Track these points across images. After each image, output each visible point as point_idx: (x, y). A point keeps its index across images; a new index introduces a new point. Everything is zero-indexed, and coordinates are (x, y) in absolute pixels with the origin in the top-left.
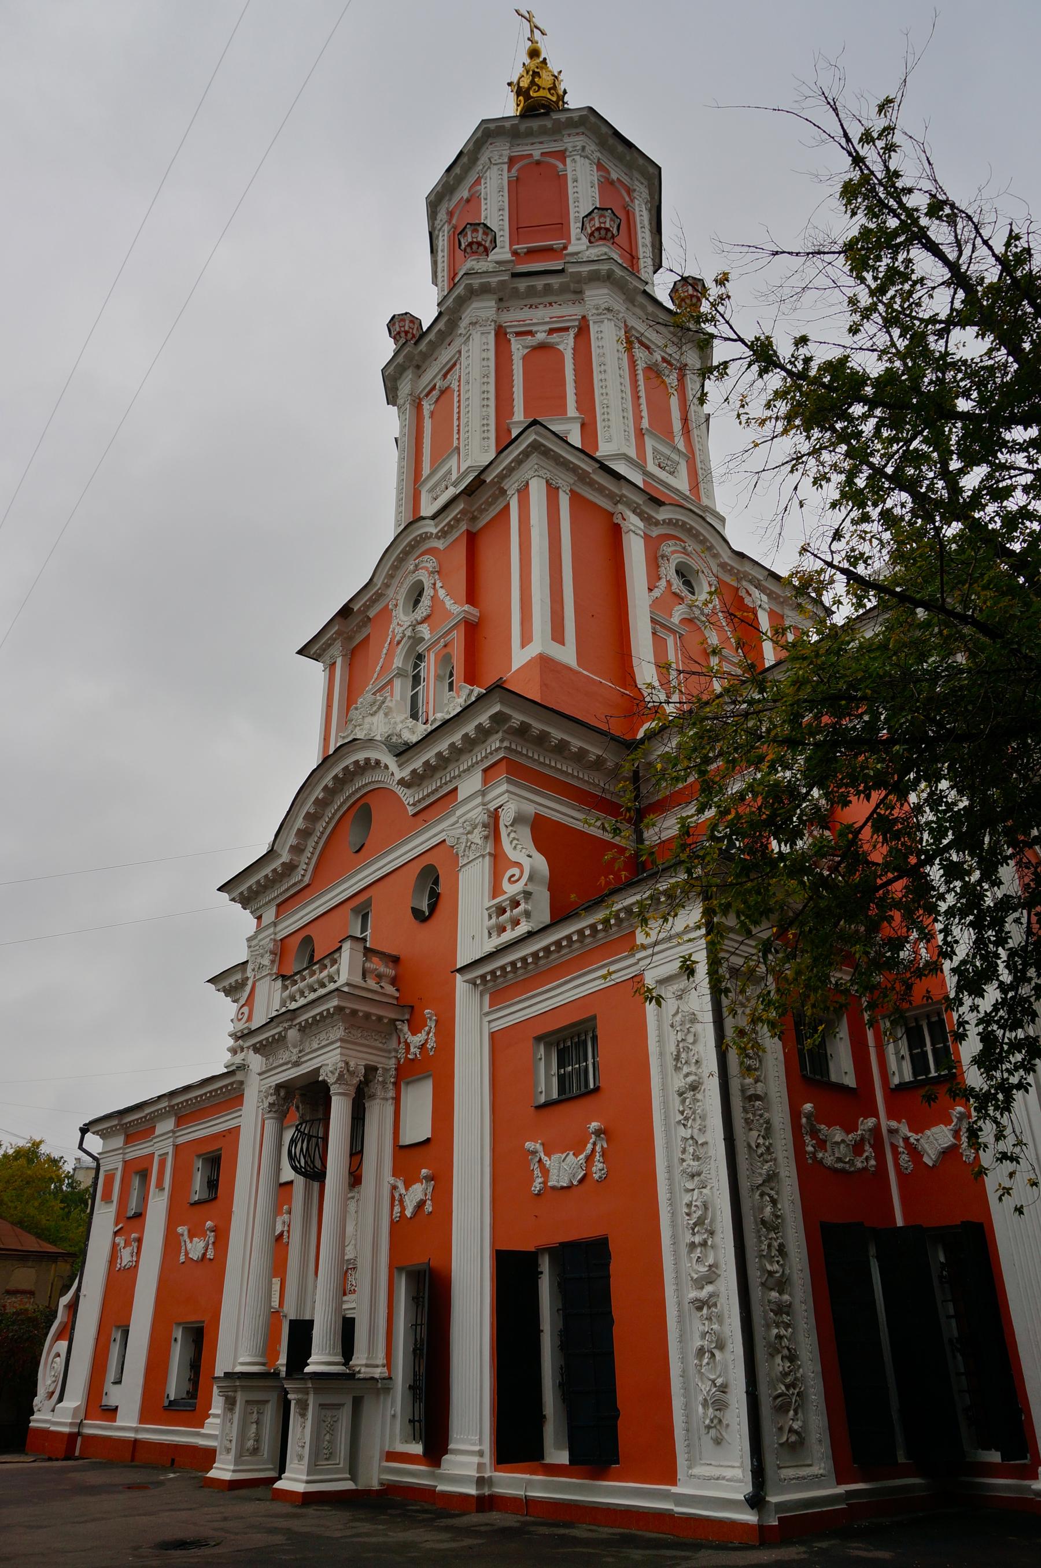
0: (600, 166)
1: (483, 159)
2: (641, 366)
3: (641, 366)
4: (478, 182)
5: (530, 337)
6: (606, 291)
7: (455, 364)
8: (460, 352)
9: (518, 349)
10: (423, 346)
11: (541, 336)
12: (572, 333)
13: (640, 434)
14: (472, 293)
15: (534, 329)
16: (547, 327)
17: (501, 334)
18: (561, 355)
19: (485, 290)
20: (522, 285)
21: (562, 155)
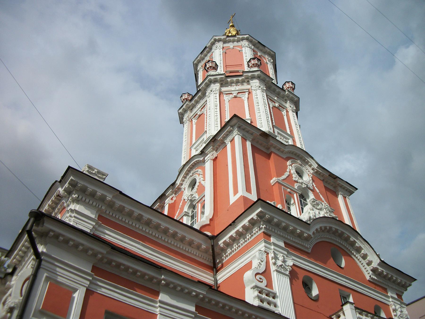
0: (254, 51)
1: (214, 47)
2: (271, 106)
3: (271, 106)
4: (212, 54)
5: (231, 95)
6: (258, 81)
7: (205, 106)
8: (206, 101)
9: (226, 98)
10: (193, 102)
11: (234, 94)
12: (247, 93)
13: (273, 126)
14: (211, 82)
15: (233, 92)
16: (237, 92)
17: (221, 93)
18: (243, 101)
19: (215, 81)
20: (229, 80)
21: (241, 47)
